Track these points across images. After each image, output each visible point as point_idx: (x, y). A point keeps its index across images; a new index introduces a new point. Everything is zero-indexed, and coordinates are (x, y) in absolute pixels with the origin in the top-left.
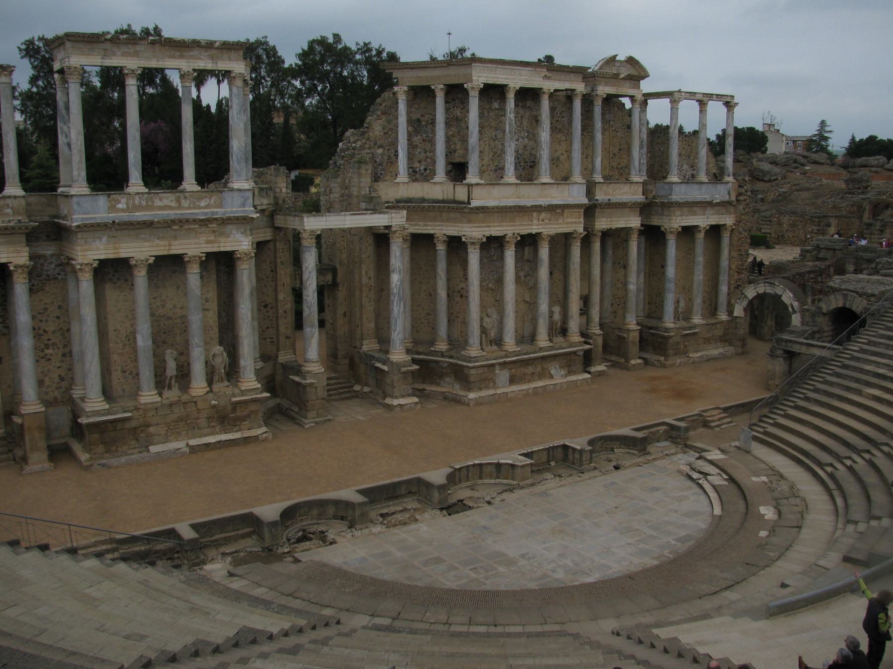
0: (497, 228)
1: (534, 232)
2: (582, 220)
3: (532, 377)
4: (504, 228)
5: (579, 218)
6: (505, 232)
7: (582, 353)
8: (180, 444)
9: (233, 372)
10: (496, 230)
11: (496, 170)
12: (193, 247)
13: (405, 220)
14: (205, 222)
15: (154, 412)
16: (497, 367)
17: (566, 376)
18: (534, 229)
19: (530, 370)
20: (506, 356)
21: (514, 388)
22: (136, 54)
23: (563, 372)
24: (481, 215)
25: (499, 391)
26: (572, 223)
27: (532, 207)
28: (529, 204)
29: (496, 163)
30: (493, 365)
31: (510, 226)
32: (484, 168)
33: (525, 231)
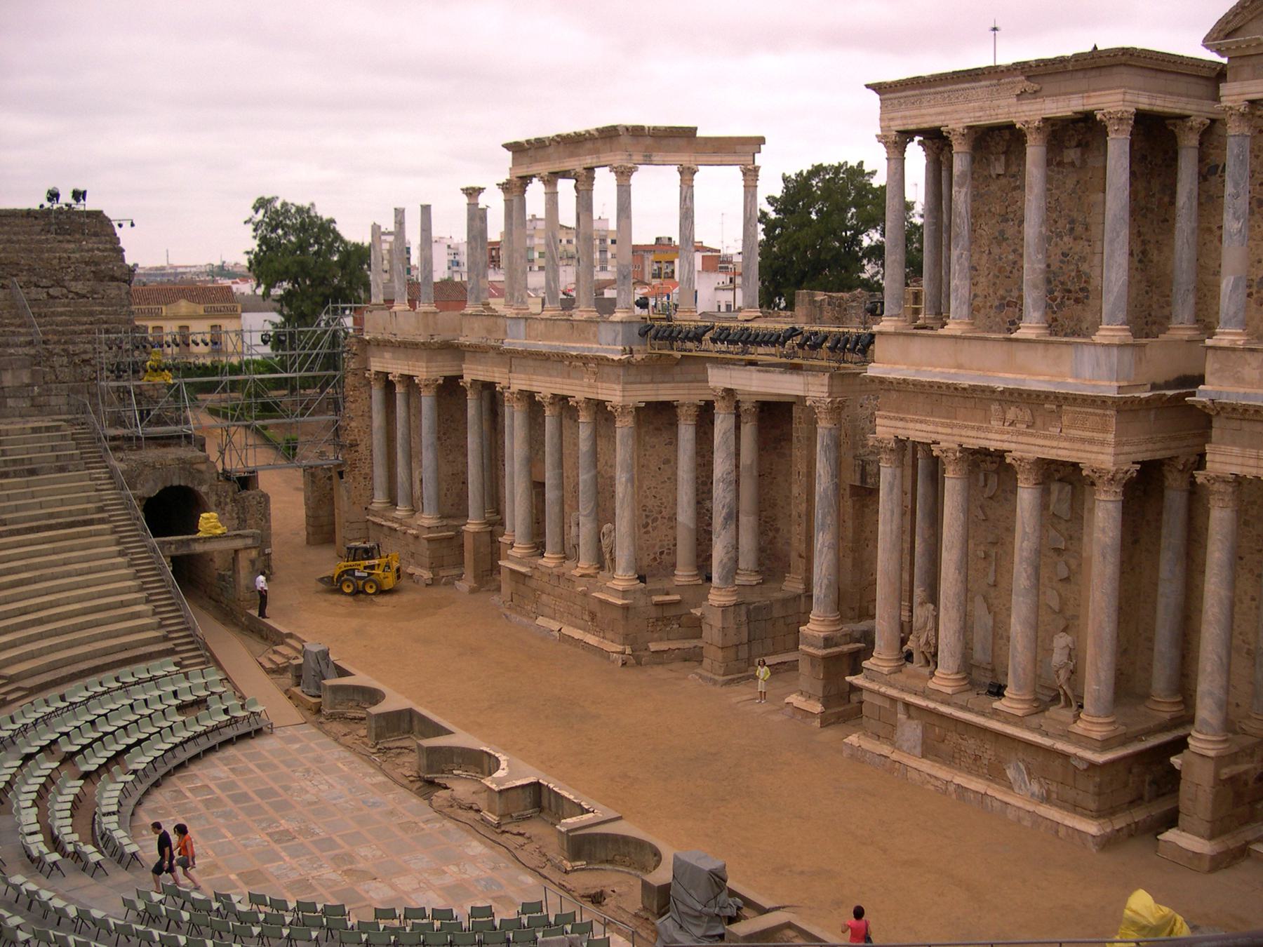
0: (918, 426)
1: (993, 445)
2: (1111, 437)
3: (975, 766)
4: (930, 428)
5: (1105, 431)
6: (935, 437)
7: (1082, 766)
8: (555, 626)
9: (603, 561)
10: (918, 430)
11: (1001, 307)
12: (579, 389)
13: (826, 389)
14: (585, 360)
15: (546, 579)
16: (900, 707)
17: (1046, 799)
18: (993, 441)
19: (971, 744)
20: (924, 694)
21: (926, 766)
22: (547, 159)
23: (1035, 787)
24: (894, 395)
25: (894, 756)
26: (1083, 440)
27: (974, 389)
28: (966, 382)
29: (1001, 292)
30: (893, 700)
31: (943, 425)
32: (979, 301)
33: (975, 440)
